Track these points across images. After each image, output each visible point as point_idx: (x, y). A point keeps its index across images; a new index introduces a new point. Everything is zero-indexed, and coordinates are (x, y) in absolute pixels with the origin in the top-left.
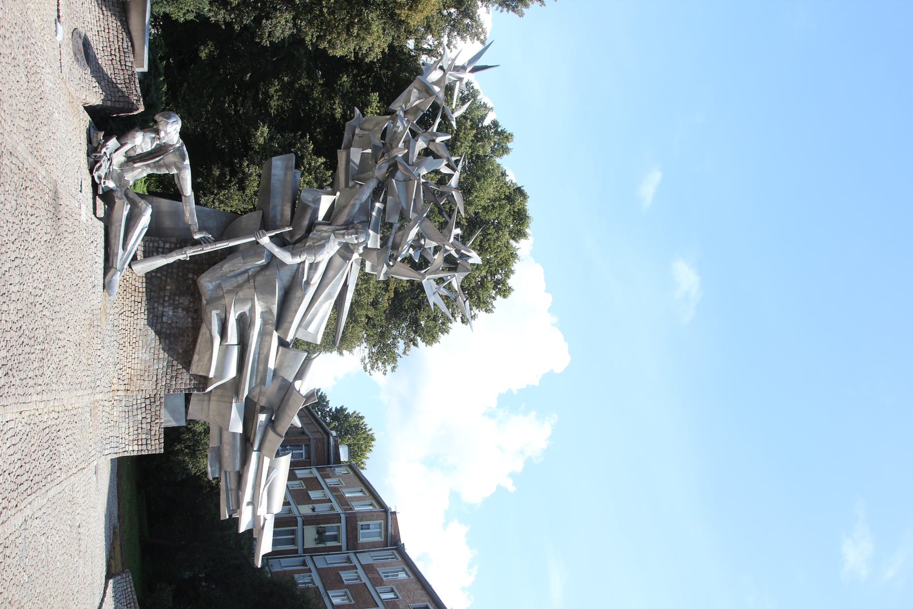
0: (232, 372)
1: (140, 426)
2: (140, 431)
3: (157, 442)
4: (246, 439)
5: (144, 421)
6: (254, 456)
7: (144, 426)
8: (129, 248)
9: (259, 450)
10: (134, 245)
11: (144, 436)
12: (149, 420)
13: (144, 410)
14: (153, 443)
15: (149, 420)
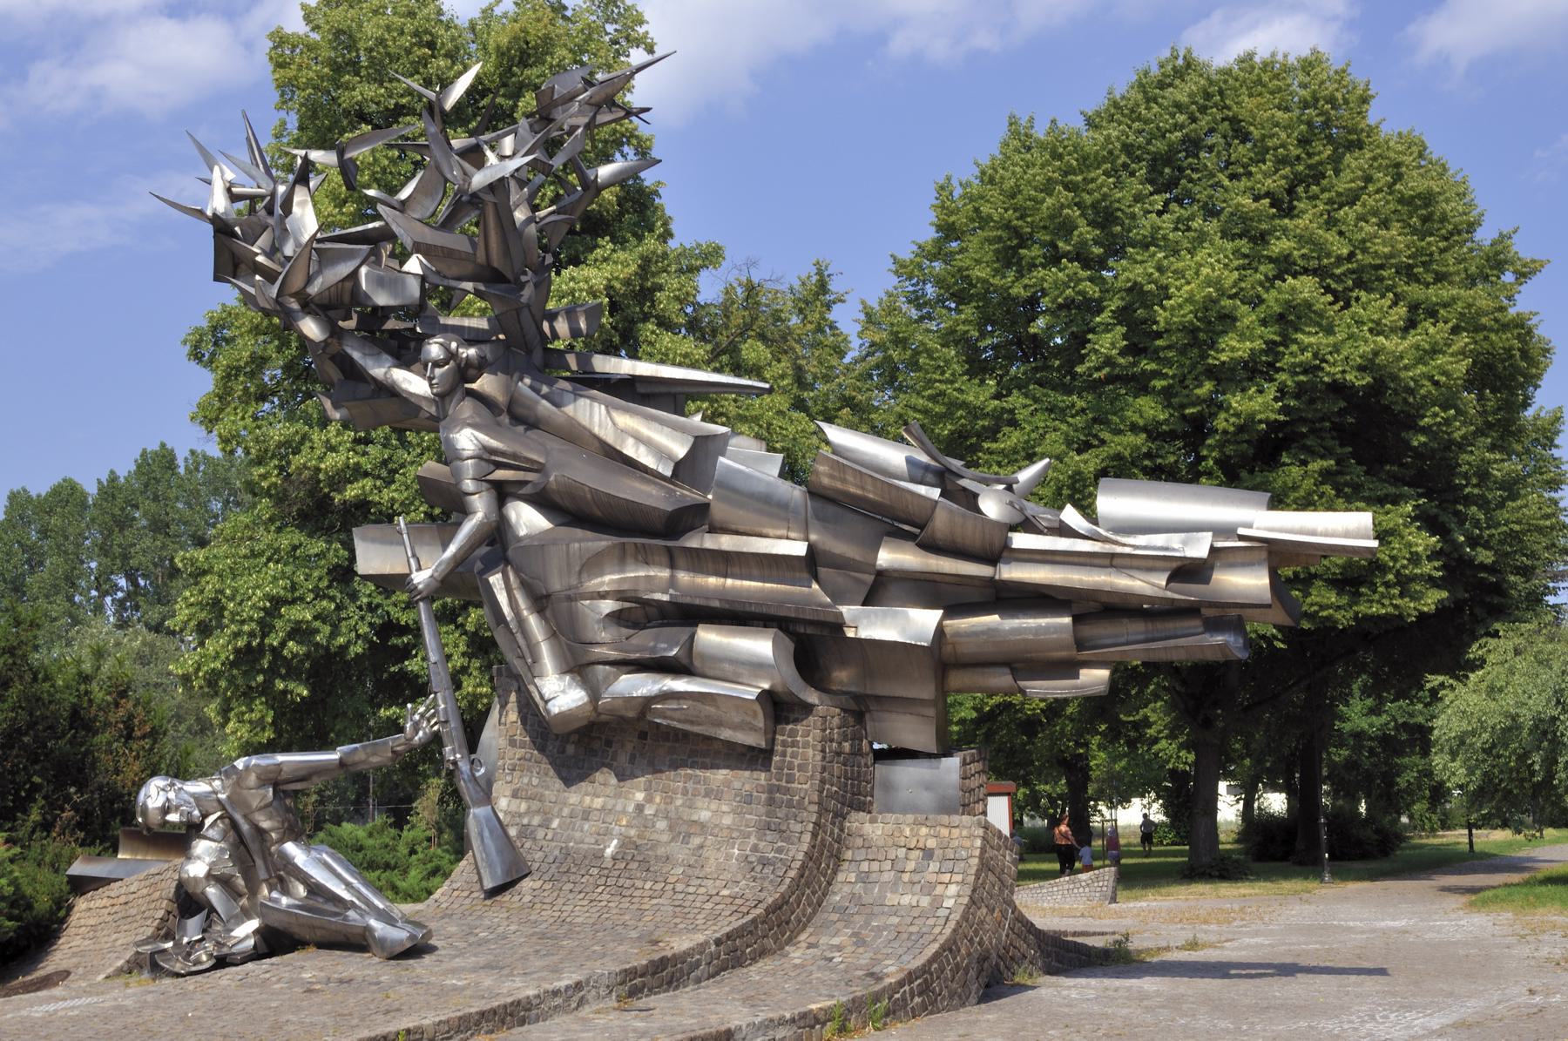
0: (760, 646)
1: (906, 877)
2: (916, 878)
3: (956, 832)
4: (954, 598)
5: (899, 866)
6: (1012, 572)
7: (911, 866)
8: (346, 896)
9: (992, 559)
10: (348, 885)
11: (934, 866)
12: (902, 852)
13: (875, 866)
14: (956, 843)
15: (902, 852)
